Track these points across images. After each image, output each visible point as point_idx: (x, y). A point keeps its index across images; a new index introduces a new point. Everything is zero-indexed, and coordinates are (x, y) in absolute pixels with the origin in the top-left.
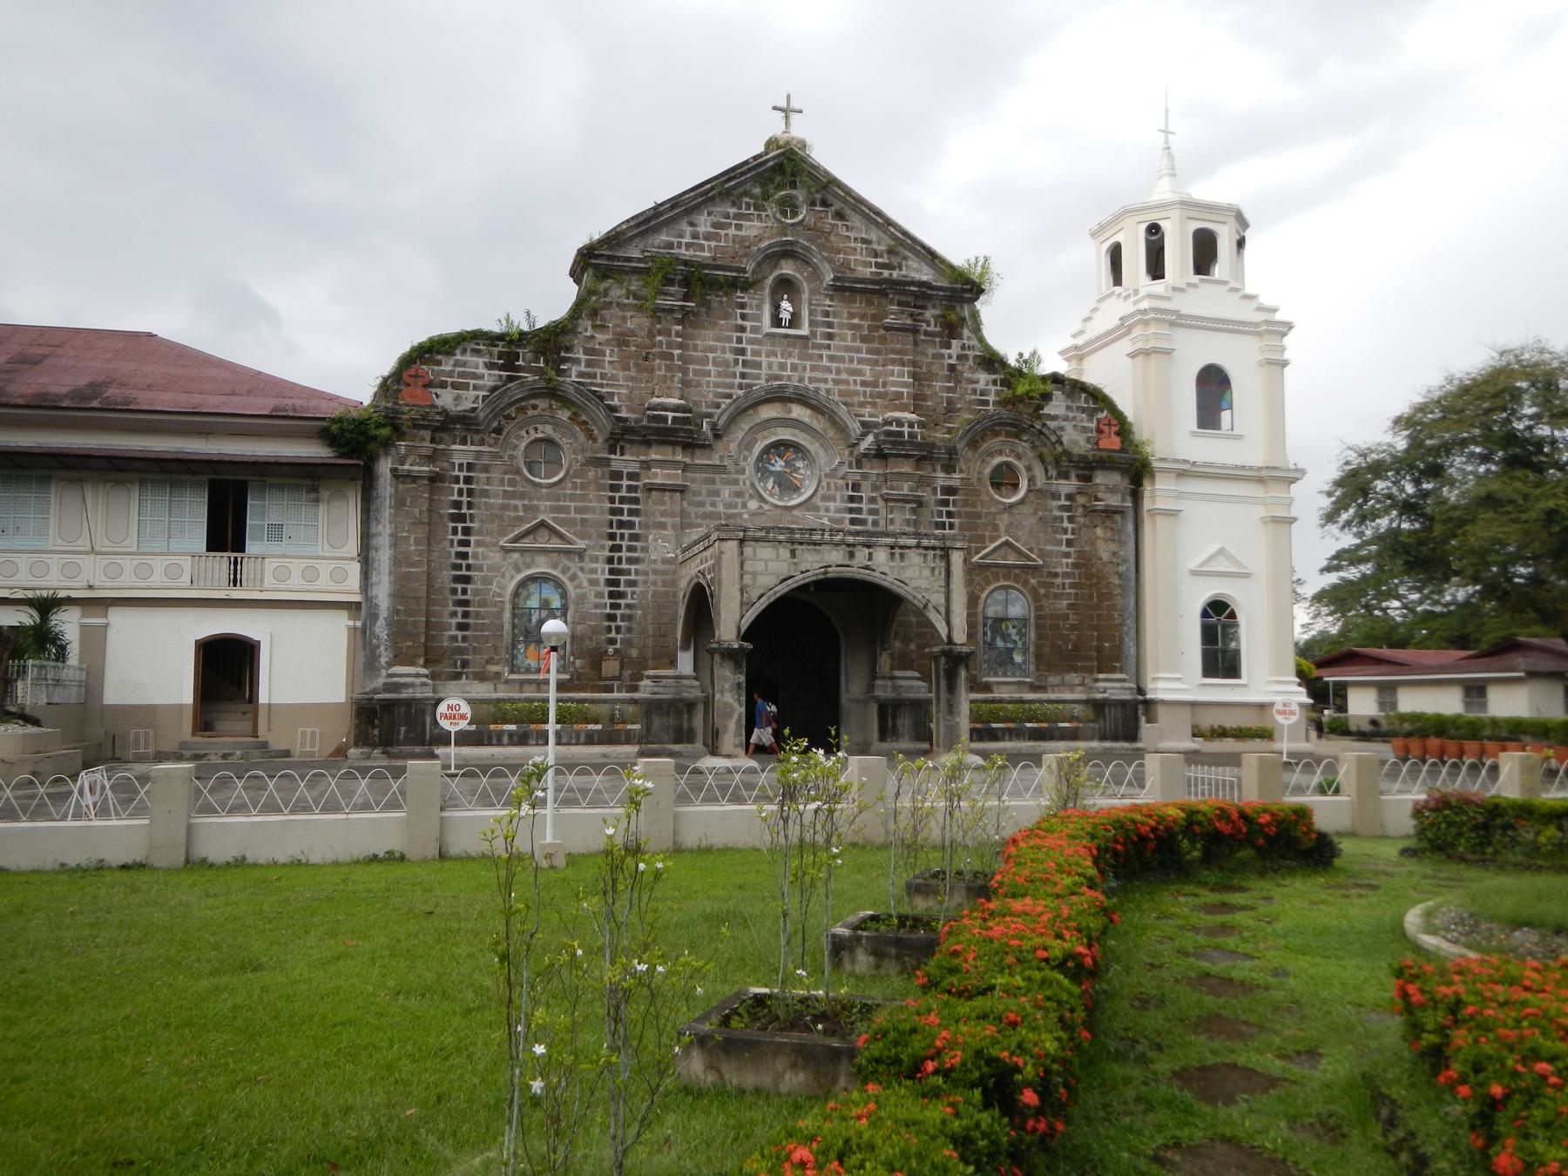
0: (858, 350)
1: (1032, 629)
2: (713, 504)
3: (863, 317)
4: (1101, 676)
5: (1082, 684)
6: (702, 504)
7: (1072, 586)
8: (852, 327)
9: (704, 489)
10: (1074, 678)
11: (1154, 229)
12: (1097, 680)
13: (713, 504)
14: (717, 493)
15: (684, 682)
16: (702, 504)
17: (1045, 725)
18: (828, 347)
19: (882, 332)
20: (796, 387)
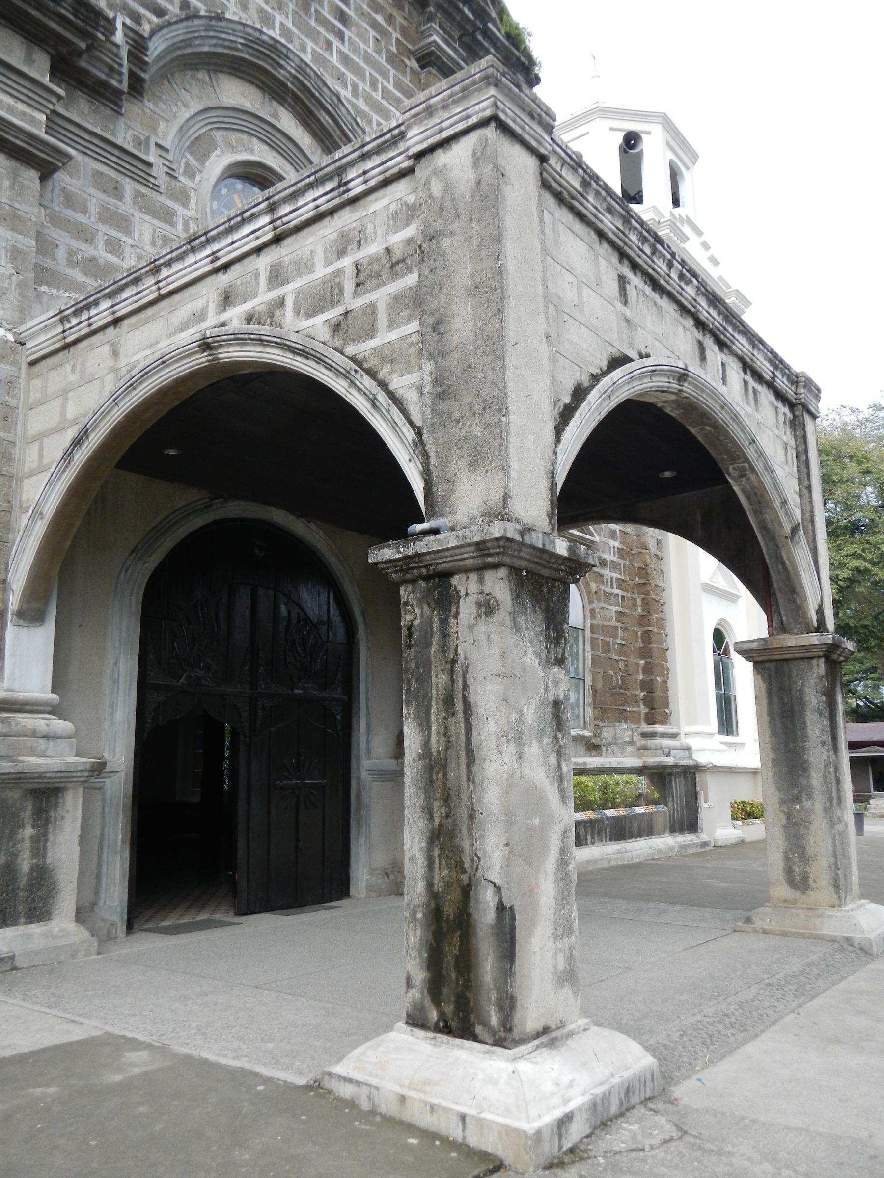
0: (385, 75)
1: (588, 647)
2: (114, 246)
3: (390, 19)
4: (659, 728)
5: (632, 743)
6: (85, 234)
7: (621, 583)
8: (375, 25)
9: (96, 199)
10: (624, 730)
11: (631, 141)
12: (653, 735)
13: (114, 246)
14: (124, 224)
15: (26, 721)
16: (85, 234)
17: (622, 812)
18: (341, 36)
19: (415, 65)
20: (303, 67)
